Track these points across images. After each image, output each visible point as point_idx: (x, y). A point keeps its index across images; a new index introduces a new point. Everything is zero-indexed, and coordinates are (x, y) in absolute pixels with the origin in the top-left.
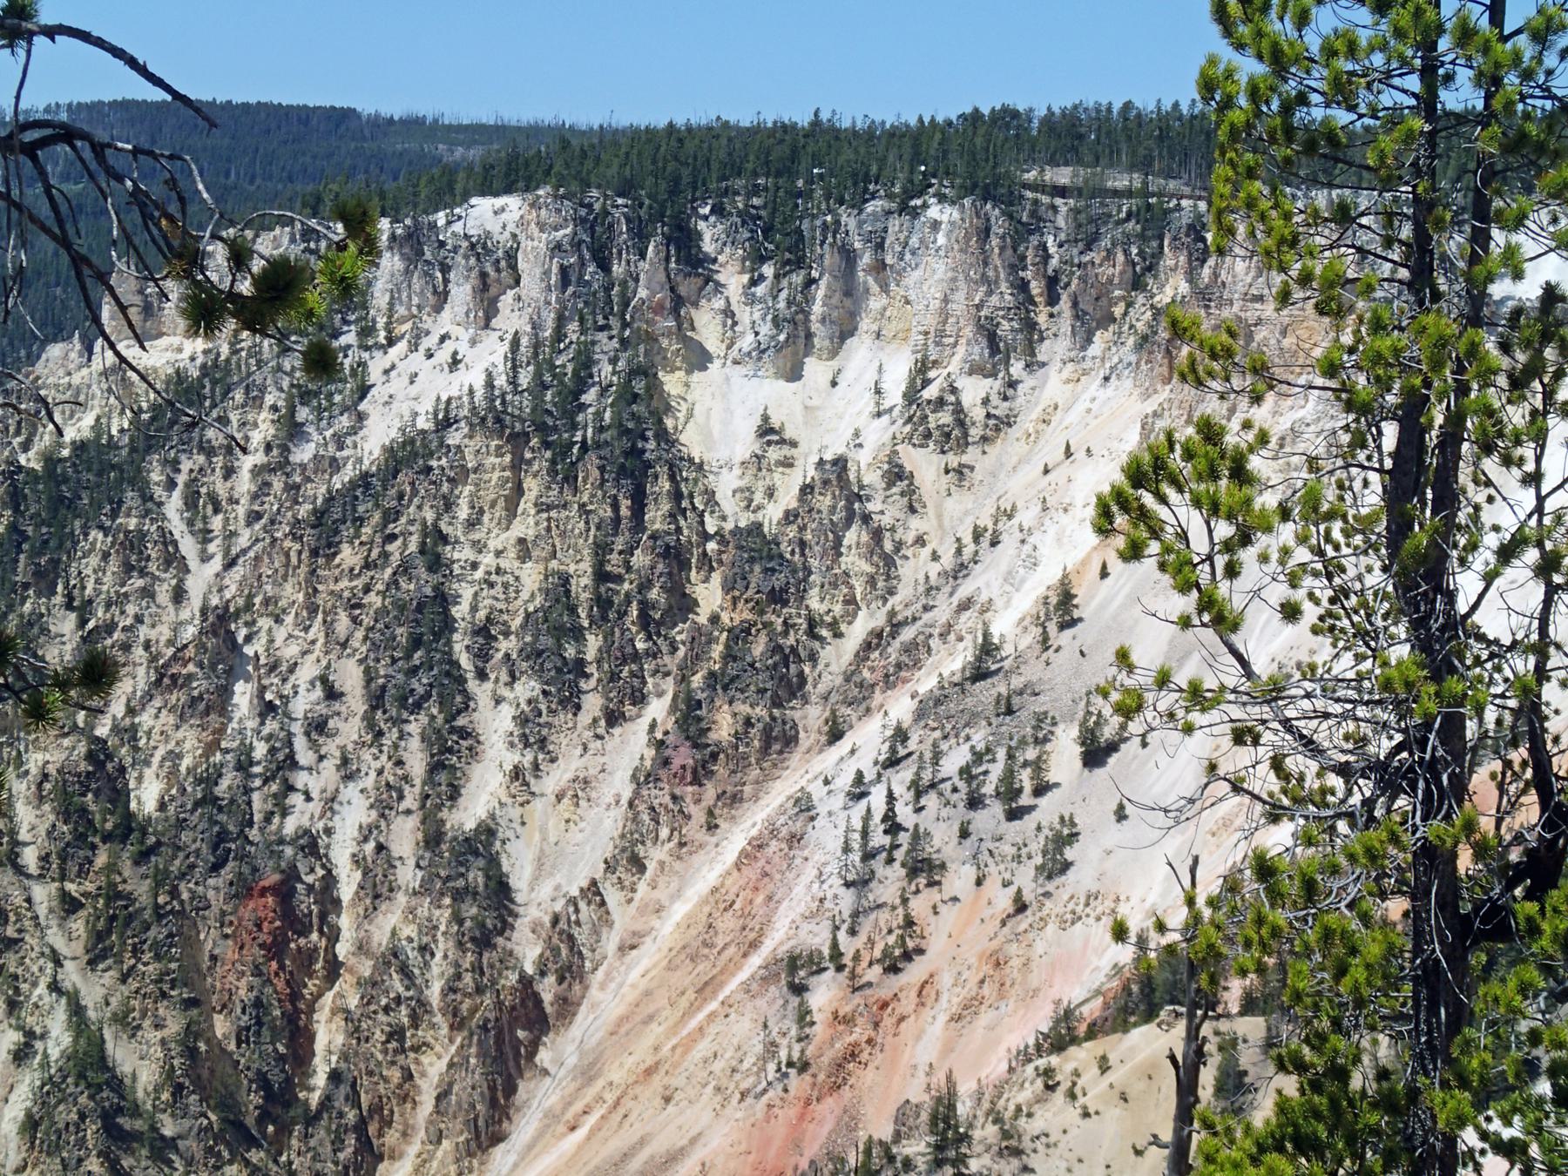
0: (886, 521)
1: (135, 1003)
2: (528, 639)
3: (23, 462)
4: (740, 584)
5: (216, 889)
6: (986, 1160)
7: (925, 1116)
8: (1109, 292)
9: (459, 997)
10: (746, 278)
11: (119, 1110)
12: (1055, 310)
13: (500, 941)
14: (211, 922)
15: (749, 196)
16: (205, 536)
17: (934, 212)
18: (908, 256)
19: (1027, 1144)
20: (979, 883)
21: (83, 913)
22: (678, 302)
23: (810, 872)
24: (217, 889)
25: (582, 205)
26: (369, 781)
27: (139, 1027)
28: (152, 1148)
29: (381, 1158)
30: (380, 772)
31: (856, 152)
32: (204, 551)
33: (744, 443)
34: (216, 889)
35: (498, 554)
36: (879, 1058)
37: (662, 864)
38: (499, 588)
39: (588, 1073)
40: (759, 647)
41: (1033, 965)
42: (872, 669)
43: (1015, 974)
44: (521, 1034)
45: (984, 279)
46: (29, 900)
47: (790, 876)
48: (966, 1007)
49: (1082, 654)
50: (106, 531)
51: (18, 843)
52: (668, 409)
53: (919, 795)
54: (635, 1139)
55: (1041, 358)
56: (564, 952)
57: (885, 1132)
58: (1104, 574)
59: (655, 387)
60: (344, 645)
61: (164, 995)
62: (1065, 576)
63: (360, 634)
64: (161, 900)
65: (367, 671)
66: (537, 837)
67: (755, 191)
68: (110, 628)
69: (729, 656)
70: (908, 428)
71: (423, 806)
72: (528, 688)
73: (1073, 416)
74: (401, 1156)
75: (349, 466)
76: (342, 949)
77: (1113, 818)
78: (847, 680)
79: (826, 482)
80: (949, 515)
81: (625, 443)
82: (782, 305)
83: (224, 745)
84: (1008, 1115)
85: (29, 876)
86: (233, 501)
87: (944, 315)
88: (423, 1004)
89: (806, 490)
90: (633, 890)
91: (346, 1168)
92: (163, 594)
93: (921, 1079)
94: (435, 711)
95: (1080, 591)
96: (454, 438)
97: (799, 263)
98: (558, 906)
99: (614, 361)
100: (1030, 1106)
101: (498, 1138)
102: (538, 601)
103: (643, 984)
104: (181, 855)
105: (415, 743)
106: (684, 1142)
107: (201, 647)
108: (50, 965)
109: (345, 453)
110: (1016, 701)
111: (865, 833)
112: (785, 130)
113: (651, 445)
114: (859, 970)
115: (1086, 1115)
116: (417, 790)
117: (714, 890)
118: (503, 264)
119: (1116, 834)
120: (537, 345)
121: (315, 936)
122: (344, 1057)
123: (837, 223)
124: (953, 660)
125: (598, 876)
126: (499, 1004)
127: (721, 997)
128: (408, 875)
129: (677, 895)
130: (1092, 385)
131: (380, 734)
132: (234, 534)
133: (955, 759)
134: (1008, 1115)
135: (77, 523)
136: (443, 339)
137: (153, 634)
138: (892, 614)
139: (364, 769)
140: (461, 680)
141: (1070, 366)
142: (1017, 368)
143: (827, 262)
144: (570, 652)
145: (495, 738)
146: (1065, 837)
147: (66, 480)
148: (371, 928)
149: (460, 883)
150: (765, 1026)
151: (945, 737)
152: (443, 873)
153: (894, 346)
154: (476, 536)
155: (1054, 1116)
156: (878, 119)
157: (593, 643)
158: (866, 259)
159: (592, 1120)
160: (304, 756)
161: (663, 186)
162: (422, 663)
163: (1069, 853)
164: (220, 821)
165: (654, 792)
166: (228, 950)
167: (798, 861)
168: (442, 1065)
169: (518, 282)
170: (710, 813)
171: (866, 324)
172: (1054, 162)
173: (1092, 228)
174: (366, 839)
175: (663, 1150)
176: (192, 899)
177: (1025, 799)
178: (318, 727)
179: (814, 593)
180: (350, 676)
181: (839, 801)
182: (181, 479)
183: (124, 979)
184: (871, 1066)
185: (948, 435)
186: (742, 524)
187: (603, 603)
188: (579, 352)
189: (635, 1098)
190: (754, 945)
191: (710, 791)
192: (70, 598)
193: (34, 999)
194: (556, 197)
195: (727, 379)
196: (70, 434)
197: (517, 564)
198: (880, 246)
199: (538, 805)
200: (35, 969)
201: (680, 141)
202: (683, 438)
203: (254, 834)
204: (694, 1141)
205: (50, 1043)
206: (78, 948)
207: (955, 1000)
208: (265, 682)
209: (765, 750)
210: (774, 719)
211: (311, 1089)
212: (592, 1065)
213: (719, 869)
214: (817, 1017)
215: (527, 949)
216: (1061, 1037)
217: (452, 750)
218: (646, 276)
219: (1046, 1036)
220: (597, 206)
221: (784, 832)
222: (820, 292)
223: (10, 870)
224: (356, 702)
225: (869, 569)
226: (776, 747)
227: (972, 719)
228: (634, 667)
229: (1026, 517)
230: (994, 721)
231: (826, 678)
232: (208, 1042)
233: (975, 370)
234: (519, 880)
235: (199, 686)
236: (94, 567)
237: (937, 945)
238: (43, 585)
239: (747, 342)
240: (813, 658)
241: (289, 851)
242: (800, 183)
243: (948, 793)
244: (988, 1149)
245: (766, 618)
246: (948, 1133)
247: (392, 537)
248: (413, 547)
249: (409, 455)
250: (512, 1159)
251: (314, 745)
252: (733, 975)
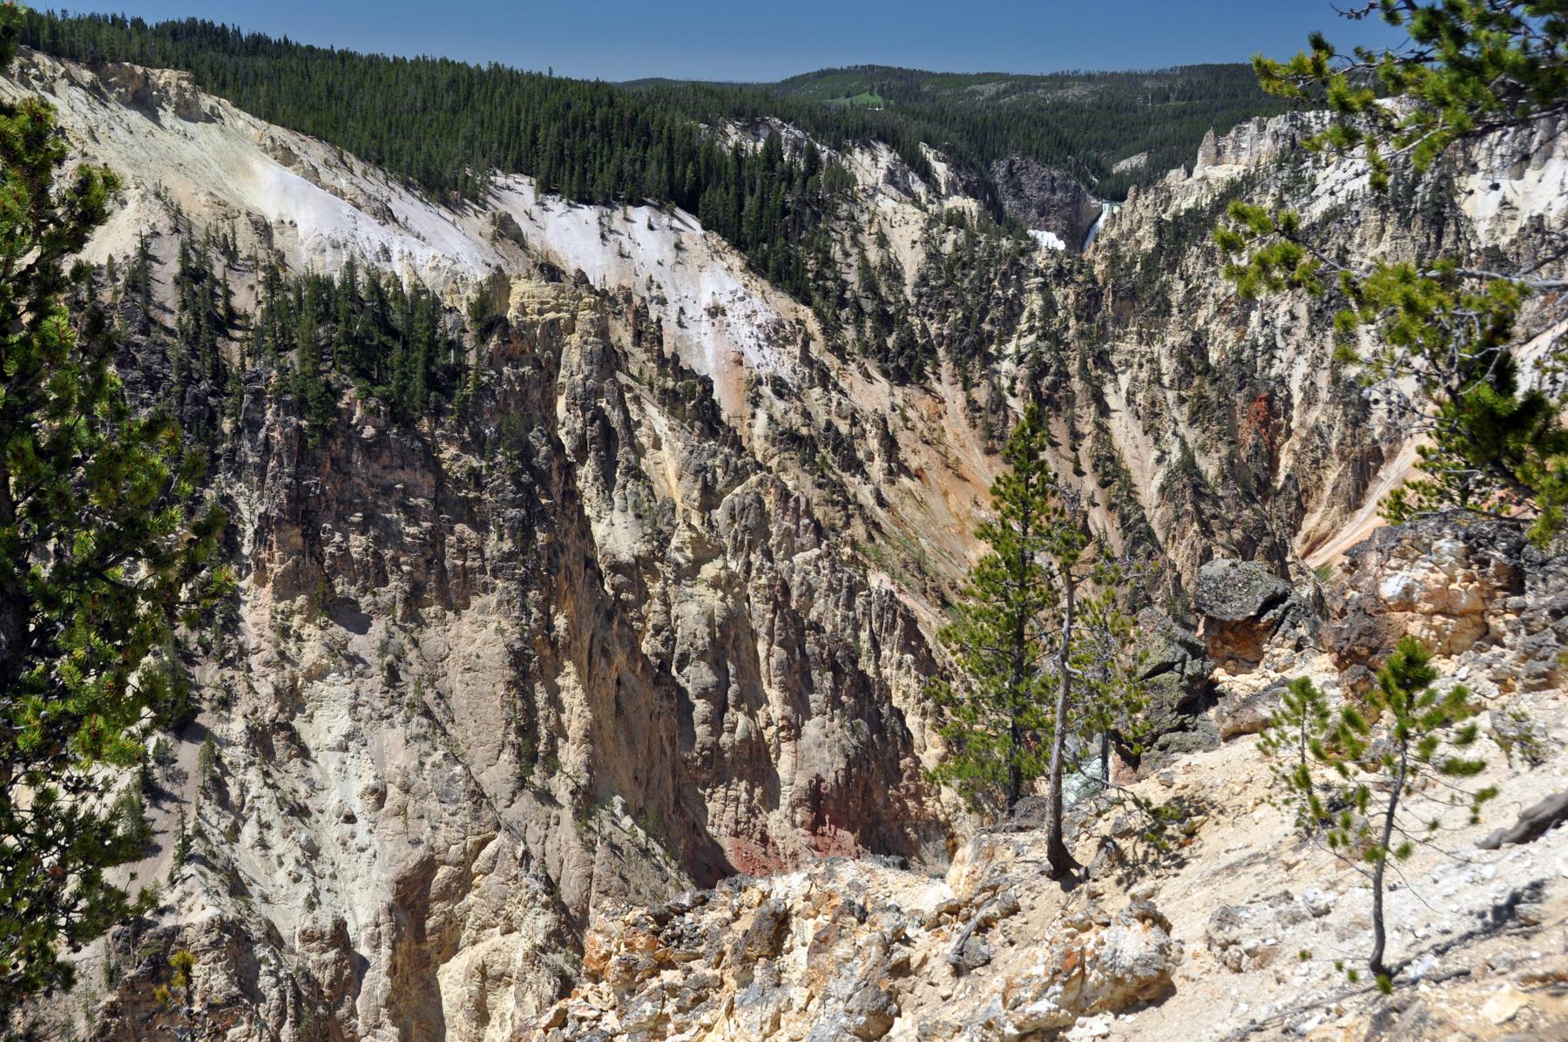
5: (1239, 399)
26: (1309, 355)
68: (1198, 288)
76: (1293, 425)
88: (1328, 449)
96: (1355, 207)
101: (1359, 507)
105: (1330, 340)
107: (1237, 296)
122: (1293, 469)
128: (1324, 395)
160: (1280, 343)
164: (1243, 370)
168: (1335, 475)
178: (1287, 332)
180: (1302, 310)
196: (1184, 206)
224: (1304, 320)
235: (1236, 313)
236: (1192, 261)
249: (1333, 215)
251: (1285, 339)
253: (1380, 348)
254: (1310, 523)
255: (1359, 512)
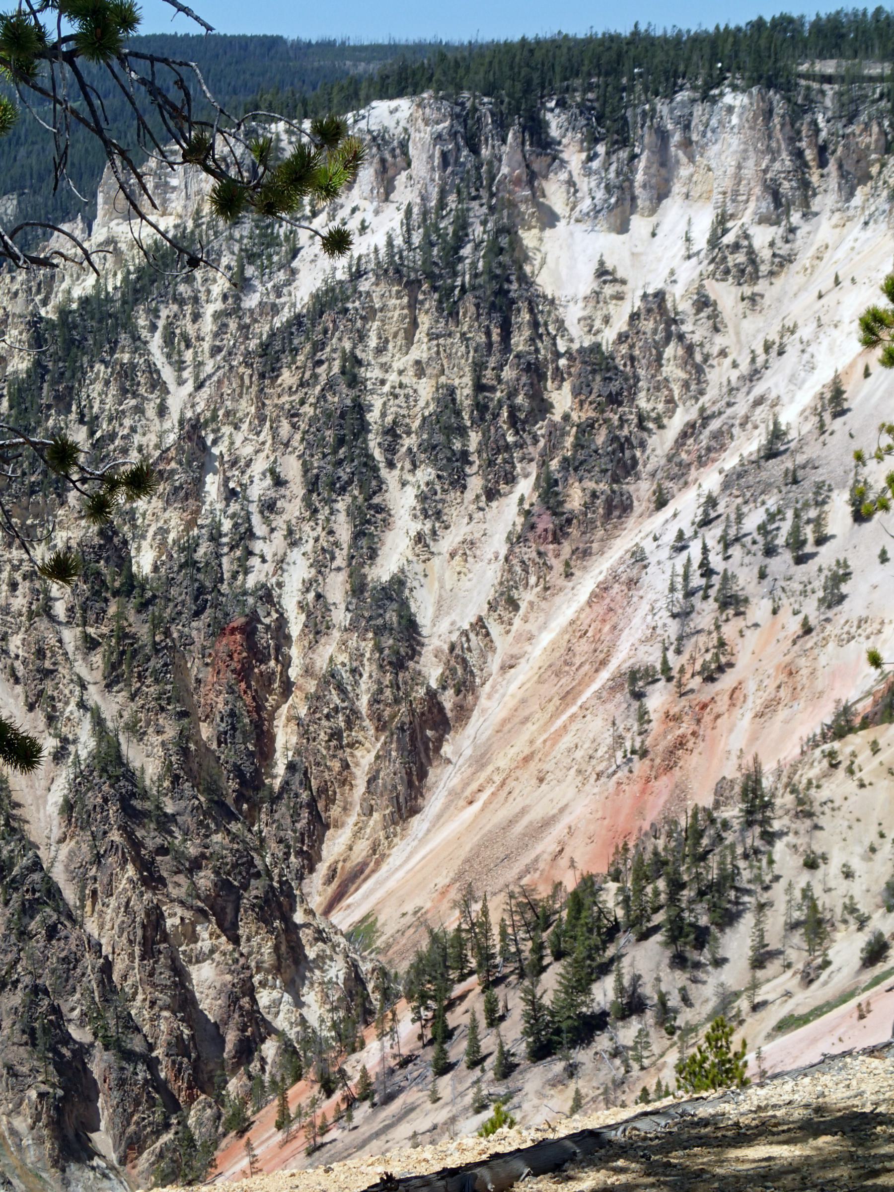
0: (696, 338)
1: (141, 715)
2: (425, 436)
3: (43, 312)
4: (585, 390)
5: (197, 630)
6: (786, 821)
7: (737, 789)
8: (867, 156)
9: (381, 706)
10: (584, 155)
11: (133, 795)
12: (825, 171)
13: (411, 664)
14: (195, 655)
15: (585, 92)
16: (180, 366)
17: (729, 98)
18: (709, 134)
19: (816, 808)
20: (775, 612)
21: (100, 650)
22: (532, 177)
23: (645, 607)
24: (198, 629)
25: (457, 104)
26: (309, 547)
27: (145, 733)
28: (158, 823)
29: (327, 827)
30: (317, 540)
31: (667, 54)
32: (179, 377)
33: (586, 284)
34: (197, 630)
35: (401, 372)
36: (701, 745)
37: (531, 604)
38: (402, 399)
39: (480, 761)
40: (601, 438)
41: (819, 673)
42: (688, 452)
43: (805, 680)
44: (429, 733)
45: (769, 150)
46: (60, 641)
47: (629, 610)
48: (767, 707)
49: (851, 436)
50: (106, 364)
51: (51, 599)
52: (527, 258)
53: (727, 546)
54: (517, 810)
55: (814, 209)
56: (460, 672)
57: (707, 801)
58: (867, 374)
59: (516, 242)
60: (287, 445)
61: (163, 709)
62: (837, 377)
63: (298, 436)
64: (157, 639)
65: (304, 464)
66: (436, 585)
67: (590, 88)
68: (112, 436)
69: (578, 445)
70: (712, 267)
71: (349, 565)
72: (426, 474)
73: (841, 254)
74: (343, 825)
75: (286, 310)
76: (293, 673)
77: (878, 561)
78: (670, 459)
79: (649, 311)
80: (743, 334)
81: (495, 286)
82: (612, 175)
83: (199, 522)
84: (802, 787)
85: (60, 623)
86: (200, 339)
87: (738, 179)
88: (355, 712)
89: (634, 317)
90: (510, 624)
91: (302, 834)
92: (151, 411)
93: (734, 761)
94: (356, 493)
95: (848, 388)
96: (364, 286)
97: (625, 142)
98: (454, 637)
99: (484, 223)
100: (818, 779)
101: (414, 811)
102: (432, 407)
103: (520, 694)
104: (171, 605)
105: (342, 517)
106: (555, 811)
107: (180, 449)
108: (78, 689)
109: (283, 300)
110: (800, 474)
111: (686, 577)
112: (612, 39)
113: (515, 286)
114: (684, 680)
115: (862, 786)
116: (345, 552)
117: (572, 623)
118: (398, 151)
119: (879, 573)
120: (425, 213)
121: (272, 663)
122: (298, 752)
123: (653, 110)
124: (750, 444)
125: (484, 613)
126: (412, 711)
127: (579, 703)
128: (340, 616)
129: (544, 626)
130: (855, 230)
131: (316, 511)
132: (201, 364)
133: (754, 519)
134: (802, 787)
135: (85, 359)
136: (354, 210)
137: (144, 441)
138: (702, 410)
139: (305, 538)
140: (376, 469)
141: (837, 215)
142: (796, 218)
143: (647, 139)
144: (457, 445)
145: (402, 512)
146: (840, 576)
147: (75, 327)
148: (315, 656)
149: (380, 621)
150: (614, 724)
151: (746, 502)
152: (366, 614)
153: (699, 204)
154: (383, 360)
155: (837, 787)
156: (684, 28)
157: (474, 438)
158: (677, 138)
159: (484, 796)
160: (260, 529)
161: (519, 86)
162: (344, 458)
163: (844, 588)
164: (199, 580)
165: (524, 549)
166: (208, 674)
167: (635, 599)
169: (409, 165)
170: (567, 564)
171: (677, 188)
172: (821, 56)
173: (852, 107)
174: (308, 590)
175: (539, 817)
176: (181, 637)
177: (809, 548)
178: (269, 507)
179: (642, 395)
180: (292, 468)
181: (665, 552)
182: (161, 323)
183: (132, 698)
184: (696, 752)
185: (743, 271)
186: (586, 344)
187: (481, 408)
188: (457, 218)
189: (517, 779)
190: (604, 663)
191: (566, 548)
192: (82, 415)
193: (67, 714)
194: (436, 98)
195: (571, 234)
196: (77, 293)
197: (415, 380)
198: (687, 127)
199: (436, 561)
200: (67, 692)
201: (531, 51)
202: (539, 280)
203: (224, 588)
204: (562, 810)
205: (80, 746)
206: (98, 675)
207: (759, 701)
208: (229, 474)
209: (608, 515)
210: (613, 492)
211: (274, 777)
212: (483, 755)
213: (575, 606)
214: (653, 716)
215: (432, 670)
216: (842, 726)
217: (370, 522)
218: (507, 155)
219: (829, 727)
220: (468, 105)
221: (624, 577)
222: (641, 164)
223: (45, 619)
224: (297, 487)
225: (684, 376)
226: (616, 513)
227: (766, 488)
228: (506, 455)
229: (805, 332)
230: (784, 490)
231: (653, 460)
232: (196, 743)
233: (763, 220)
234: (424, 617)
235: (180, 478)
236: (98, 391)
237: (743, 660)
238: (61, 406)
239: (586, 205)
240: (643, 445)
241: (251, 600)
242: (624, 81)
243: (749, 545)
244: (787, 812)
245: (606, 415)
246: (756, 803)
247: (320, 363)
248: (336, 369)
249: (330, 300)
250: (425, 826)
251: (267, 521)
252: (588, 686)
253: (428, 525)
254: (334, 846)
255: (415, 820)
